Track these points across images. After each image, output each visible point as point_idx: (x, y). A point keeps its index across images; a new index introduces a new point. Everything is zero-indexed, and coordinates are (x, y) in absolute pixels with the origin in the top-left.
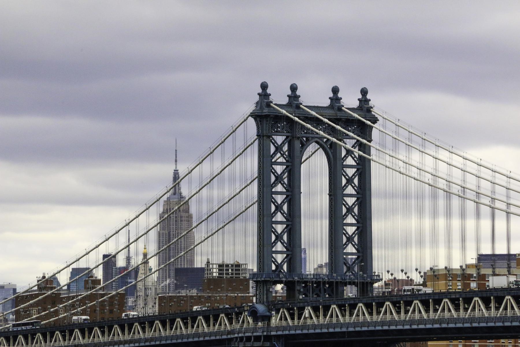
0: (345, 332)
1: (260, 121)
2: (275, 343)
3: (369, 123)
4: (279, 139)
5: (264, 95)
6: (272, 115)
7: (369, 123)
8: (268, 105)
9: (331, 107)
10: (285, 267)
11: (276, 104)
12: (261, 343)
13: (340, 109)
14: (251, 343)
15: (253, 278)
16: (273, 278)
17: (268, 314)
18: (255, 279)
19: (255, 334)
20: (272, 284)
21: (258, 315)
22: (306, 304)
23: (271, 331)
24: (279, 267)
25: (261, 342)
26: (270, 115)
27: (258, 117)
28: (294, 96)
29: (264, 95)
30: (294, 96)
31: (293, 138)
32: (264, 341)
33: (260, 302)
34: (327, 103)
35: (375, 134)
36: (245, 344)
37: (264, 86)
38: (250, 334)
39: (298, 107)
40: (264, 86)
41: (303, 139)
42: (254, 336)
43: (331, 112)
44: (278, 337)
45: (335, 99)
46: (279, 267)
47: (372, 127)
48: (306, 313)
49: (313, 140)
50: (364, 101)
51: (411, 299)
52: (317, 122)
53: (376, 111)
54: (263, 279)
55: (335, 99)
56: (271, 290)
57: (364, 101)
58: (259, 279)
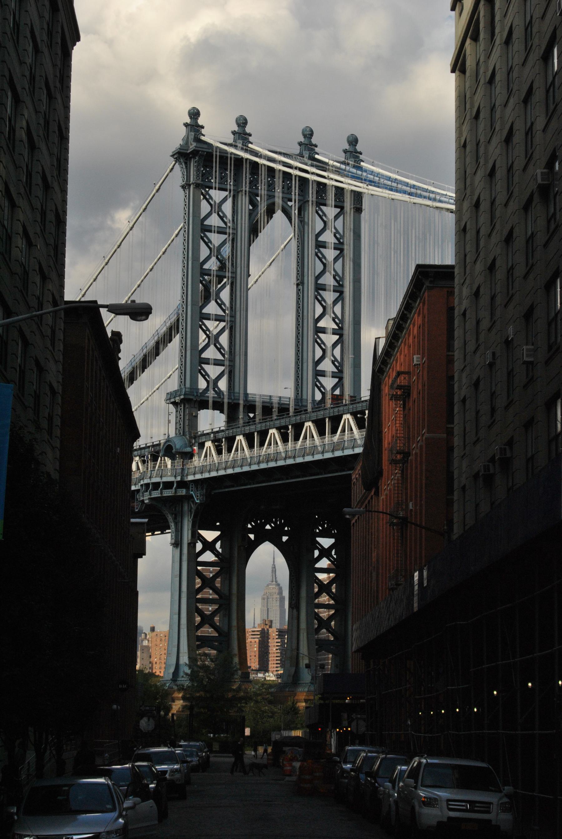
1: (186, 163)
2: (192, 493)
4: (217, 195)
6: (202, 151)
8: (198, 140)
10: (223, 385)
12: (173, 490)
14: (159, 491)
15: (170, 399)
16: (197, 395)
17: (188, 449)
18: (172, 400)
19: (165, 479)
20: (196, 406)
21: (174, 451)
23: (187, 475)
25: (172, 489)
26: (198, 151)
27: (182, 156)
33: (180, 434)
36: (150, 494)
37: (195, 114)
38: (158, 480)
40: (195, 114)
41: (256, 199)
42: (164, 483)
44: (195, 482)
54: (182, 397)
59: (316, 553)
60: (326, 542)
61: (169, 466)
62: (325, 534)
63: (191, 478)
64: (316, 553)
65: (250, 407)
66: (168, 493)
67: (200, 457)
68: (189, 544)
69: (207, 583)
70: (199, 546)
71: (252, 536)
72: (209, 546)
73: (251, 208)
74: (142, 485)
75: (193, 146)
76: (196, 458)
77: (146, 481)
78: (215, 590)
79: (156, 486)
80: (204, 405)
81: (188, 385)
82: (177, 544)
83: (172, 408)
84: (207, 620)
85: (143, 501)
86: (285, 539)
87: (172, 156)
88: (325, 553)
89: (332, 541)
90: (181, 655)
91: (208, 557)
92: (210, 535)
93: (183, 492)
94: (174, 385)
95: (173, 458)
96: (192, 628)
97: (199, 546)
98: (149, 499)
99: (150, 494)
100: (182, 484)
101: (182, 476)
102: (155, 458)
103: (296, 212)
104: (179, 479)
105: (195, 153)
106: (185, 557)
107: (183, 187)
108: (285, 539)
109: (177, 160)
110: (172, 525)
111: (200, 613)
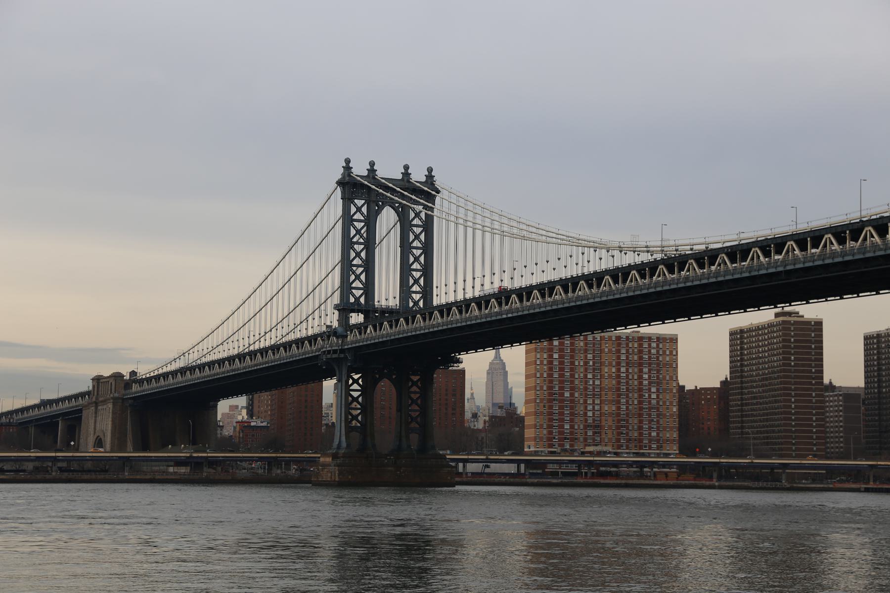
0: (388, 340)
3: (433, 193)
4: (359, 202)
5: (347, 168)
7: (433, 193)
8: (349, 175)
9: (402, 180)
10: (362, 300)
11: (356, 175)
12: (337, 355)
13: (409, 182)
17: (345, 334)
18: (337, 308)
19: (333, 348)
21: (338, 334)
22: (369, 323)
24: (357, 299)
26: (349, 182)
28: (372, 171)
29: (347, 168)
30: (372, 171)
31: (370, 201)
32: (340, 353)
34: (400, 177)
35: (438, 200)
36: (326, 356)
37: (348, 161)
38: (330, 349)
39: (374, 178)
40: (348, 161)
42: (333, 350)
43: (402, 183)
45: (406, 174)
46: (357, 299)
47: (435, 196)
48: (368, 331)
49: (389, 204)
50: (430, 177)
51: (432, 311)
52: (393, 191)
53: (438, 184)
54: (342, 307)
55: (406, 174)
56: (348, 316)
57: (430, 177)
58: (340, 308)
59: (410, 384)
60: (415, 378)
61: (336, 341)
62: (415, 374)
63: (346, 347)
64: (410, 384)
65: (375, 310)
66: (335, 356)
67: (351, 336)
68: (345, 381)
69: (355, 399)
70: (351, 381)
71: (377, 376)
72: (355, 381)
73: (377, 208)
74: (322, 352)
75: (347, 178)
76: (349, 337)
77: (324, 350)
78: (359, 403)
79: (329, 352)
80: (353, 311)
81: (345, 301)
82: (339, 381)
83: (337, 312)
84: (355, 418)
85: (323, 359)
86: (394, 377)
87: (337, 183)
88: (414, 383)
89: (418, 377)
90: (342, 435)
91: (355, 387)
92: (356, 377)
93: (342, 356)
94: (336, 299)
95: (337, 337)
96: (348, 422)
97: (351, 381)
98: (326, 359)
99: (326, 356)
100: (342, 351)
101: (342, 346)
102: (329, 337)
103: (400, 209)
104: (340, 348)
105: (348, 183)
106: (344, 387)
107: (341, 199)
108: (394, 377)
109: (338, 185)
110: (337, 373)
111: (351, 414)
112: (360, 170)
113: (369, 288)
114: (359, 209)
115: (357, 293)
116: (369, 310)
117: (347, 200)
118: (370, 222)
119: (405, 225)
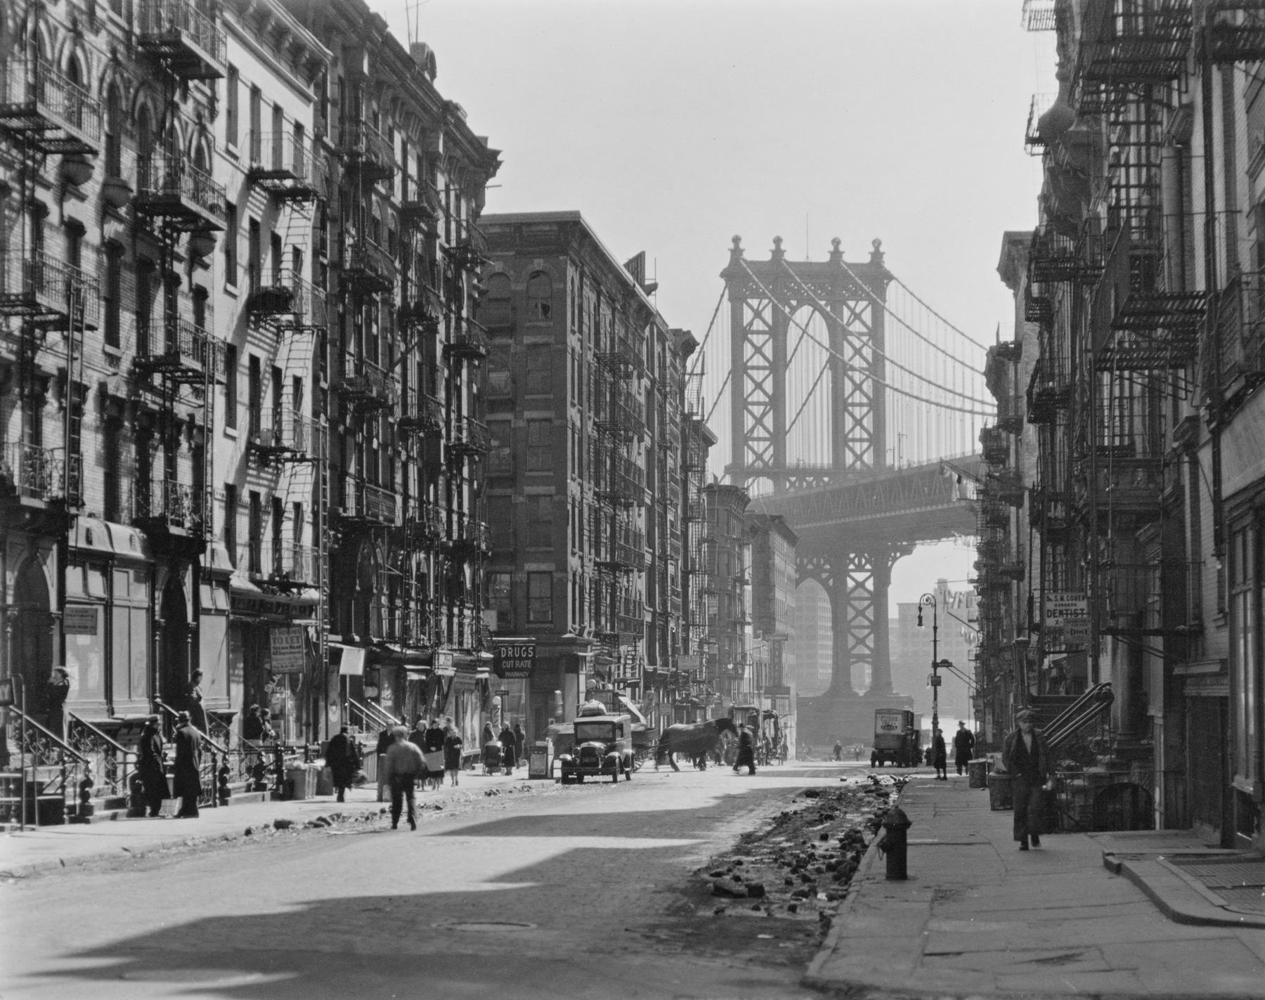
5: (736, 252)
28: (778, 253)
29: (736, 252)
37: (736, 240)
40: (736, 240)
45: (836, 254)
50: (877, 255)
53: (889, 264)
55: (836, 254)
57: (877, 255)
60: (860, 576)
86: (824, 576)
112: (756, 251)
113: (778, 437)
114: (758, 314)
115: (759, 446)
116: (777, 471)
117: (737, 301)
118: (777, 331)
119: (838, 333)
